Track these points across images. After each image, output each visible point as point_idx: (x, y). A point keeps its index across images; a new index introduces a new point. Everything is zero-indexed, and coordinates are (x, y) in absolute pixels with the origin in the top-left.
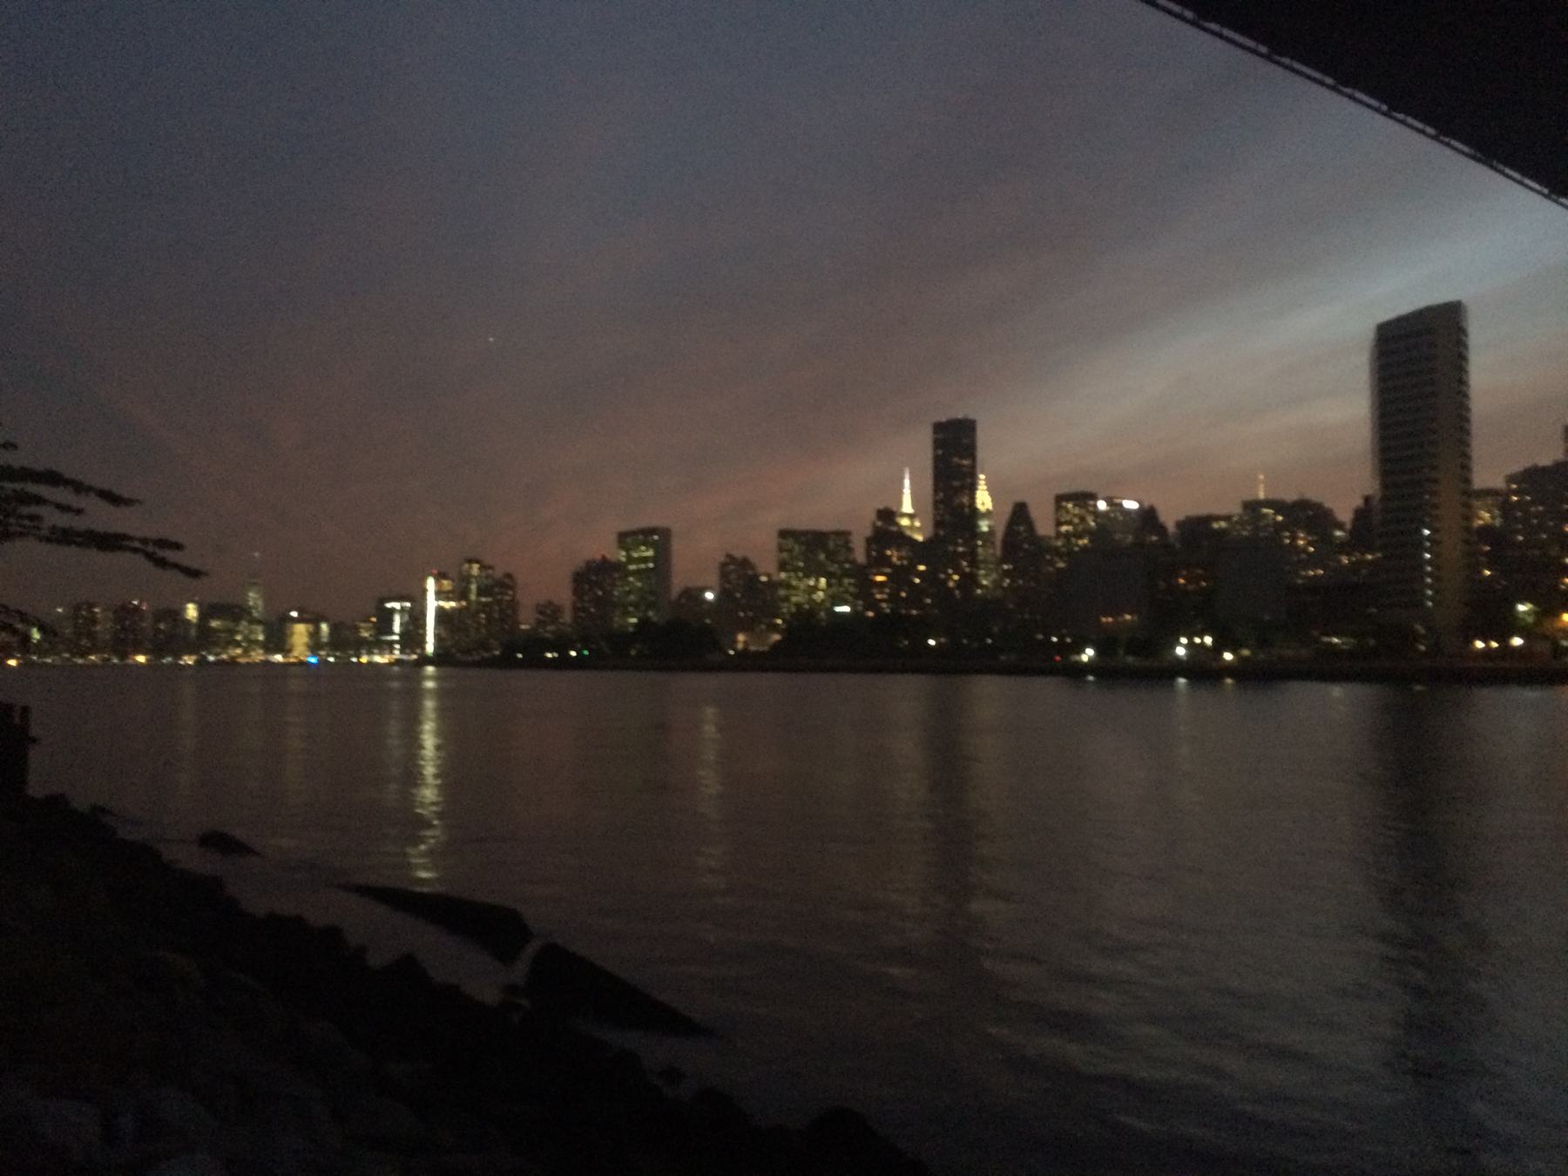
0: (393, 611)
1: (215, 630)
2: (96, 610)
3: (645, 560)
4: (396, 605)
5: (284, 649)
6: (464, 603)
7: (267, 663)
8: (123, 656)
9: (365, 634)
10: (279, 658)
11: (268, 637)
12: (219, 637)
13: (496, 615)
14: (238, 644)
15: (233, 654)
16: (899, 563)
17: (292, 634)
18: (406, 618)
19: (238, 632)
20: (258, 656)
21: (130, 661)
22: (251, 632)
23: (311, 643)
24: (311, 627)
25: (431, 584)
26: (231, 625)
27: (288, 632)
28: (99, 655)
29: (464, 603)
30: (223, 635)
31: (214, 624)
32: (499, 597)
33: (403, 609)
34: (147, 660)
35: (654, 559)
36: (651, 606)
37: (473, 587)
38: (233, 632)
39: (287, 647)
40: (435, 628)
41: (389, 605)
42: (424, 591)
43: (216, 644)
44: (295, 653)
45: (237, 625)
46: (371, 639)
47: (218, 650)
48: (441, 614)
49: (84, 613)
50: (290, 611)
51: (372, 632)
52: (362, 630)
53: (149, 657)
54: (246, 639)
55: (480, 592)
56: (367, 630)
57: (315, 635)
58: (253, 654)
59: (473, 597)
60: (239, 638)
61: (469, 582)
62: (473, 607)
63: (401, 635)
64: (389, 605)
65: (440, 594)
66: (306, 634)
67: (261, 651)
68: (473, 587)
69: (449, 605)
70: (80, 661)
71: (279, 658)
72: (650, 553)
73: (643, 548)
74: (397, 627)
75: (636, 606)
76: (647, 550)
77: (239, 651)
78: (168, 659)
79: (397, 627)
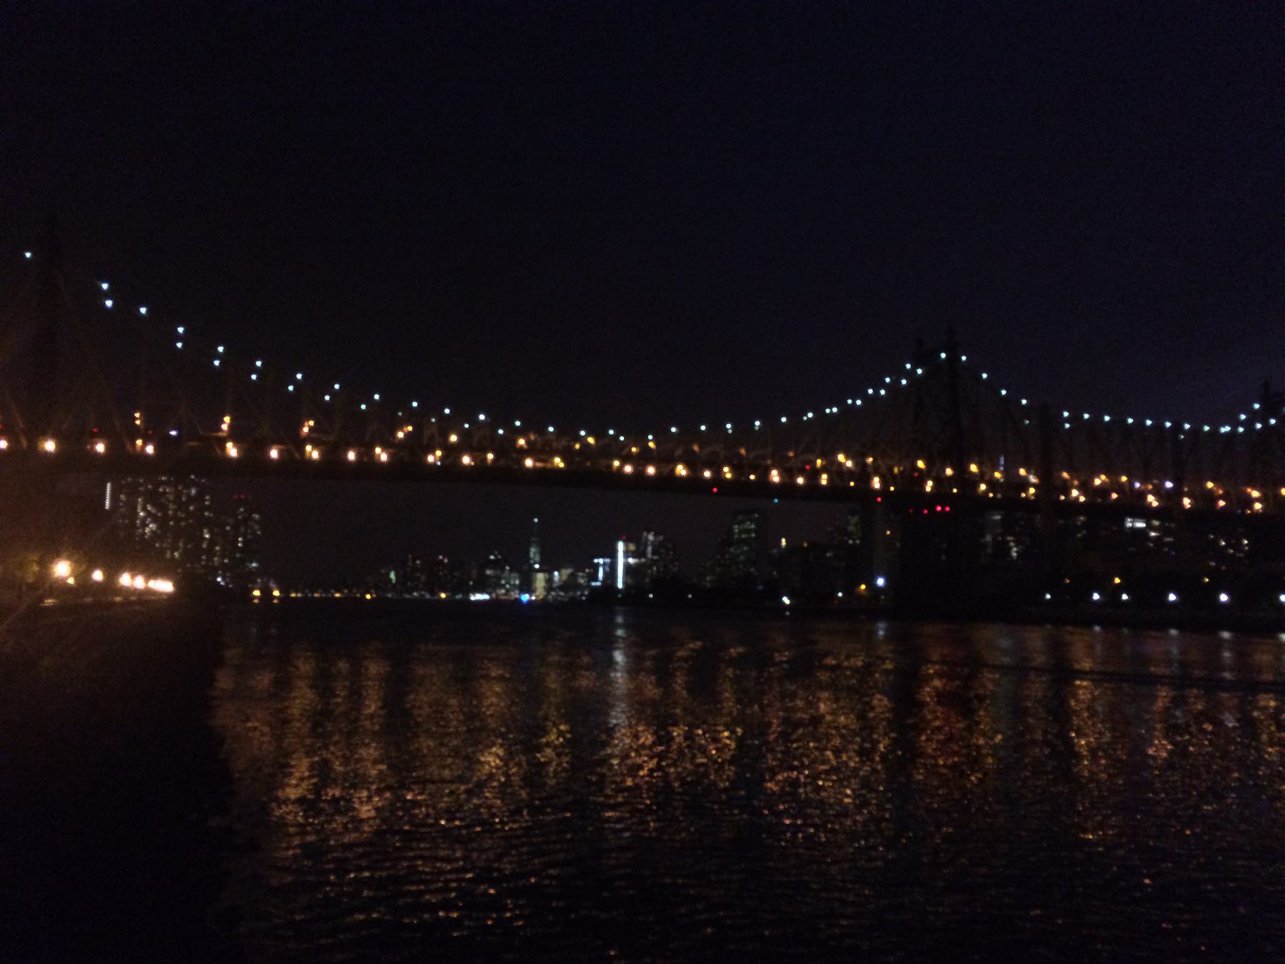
0: (598, 565)
1: (488, 577)
3: (749, 531)
4: (601, 561)
5: (530, 590)
6: (643, 560)
7: (518, 601)
9: (582, 581)
10: (525, 597)
14: (503, 586)
17: (536, 580)
18: (607, 569)
20: (515, 595)
21: (436, 597)
24: (547, 576)
25: (621, 546)
26: (499, 572)
29: (643, 560)
31: (488, 572)
33: (604, 564)
34: (447, 597)
35: (755, 531)
37: (649, 549)
38: (499, 578)
41: (596, 561)
44: (538, 593)
48: (628, 568)
51: (586, 579)
55: (654, 553)
56: (583, 577)
57: (550, 581)
58: (512, 593)
59: (649, 556)
60: (503, 582)
61: (646, 546)
63: (602, 582)
64: (596, 561)
65: (627, 554)
67: (517, 592)
68: (649, 549)
69: (631, 560)
70: (408, 596)
71: (525, 597)
72: (753, 526)
73: (749, 523)
74: (601, 574)
77: (503, 591)
78: (459, 596)
79: (601, 574)
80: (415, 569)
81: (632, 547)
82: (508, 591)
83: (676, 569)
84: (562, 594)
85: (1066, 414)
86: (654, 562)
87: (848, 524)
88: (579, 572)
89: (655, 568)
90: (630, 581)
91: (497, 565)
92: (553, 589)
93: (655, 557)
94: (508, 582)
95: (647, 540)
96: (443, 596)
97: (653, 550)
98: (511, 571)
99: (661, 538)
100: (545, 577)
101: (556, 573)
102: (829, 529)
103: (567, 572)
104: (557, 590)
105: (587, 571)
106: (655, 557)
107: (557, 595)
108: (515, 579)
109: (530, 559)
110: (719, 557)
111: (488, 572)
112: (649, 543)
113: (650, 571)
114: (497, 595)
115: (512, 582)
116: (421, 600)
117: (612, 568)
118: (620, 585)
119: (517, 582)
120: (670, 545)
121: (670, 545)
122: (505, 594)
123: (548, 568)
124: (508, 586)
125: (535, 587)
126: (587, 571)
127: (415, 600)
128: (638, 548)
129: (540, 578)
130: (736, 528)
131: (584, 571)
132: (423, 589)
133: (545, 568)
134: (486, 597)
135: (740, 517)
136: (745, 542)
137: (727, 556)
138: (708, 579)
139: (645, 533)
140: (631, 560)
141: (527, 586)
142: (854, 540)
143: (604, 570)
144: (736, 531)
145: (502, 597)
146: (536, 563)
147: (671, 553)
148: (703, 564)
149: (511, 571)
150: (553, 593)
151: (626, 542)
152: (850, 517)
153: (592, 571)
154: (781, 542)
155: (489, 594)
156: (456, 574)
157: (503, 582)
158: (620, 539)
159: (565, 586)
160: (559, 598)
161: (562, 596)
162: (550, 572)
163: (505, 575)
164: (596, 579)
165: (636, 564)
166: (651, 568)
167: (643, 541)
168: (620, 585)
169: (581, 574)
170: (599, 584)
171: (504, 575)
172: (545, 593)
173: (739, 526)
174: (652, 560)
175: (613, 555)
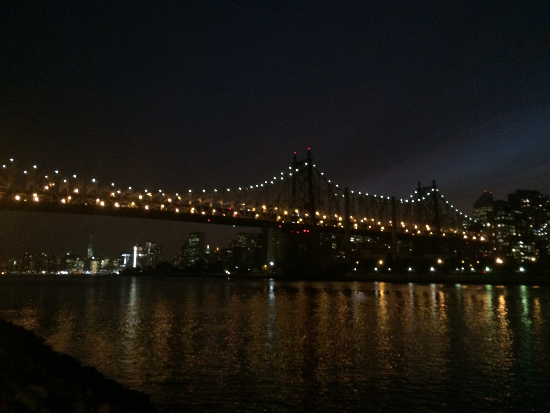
0: (124, 257)
1: (68, 263)
2: (30, 256)
4: (125, 255)
5: (89, 269)
8: (38, 271)
9: (116, 265)
10: (88, 272)
11: (85, 265)
12: (70, 265)
13: (155, 259)
14: (75, 267)
15: (73, 271)
17: (92, 264)
18: (128, 259)
20: (81, 271)
21: (40, 273)
23: (98, 268)
24: (98, 262)
25: (135, 248)
26: (73, 261)
27: (91, 264)
28: (30, 271)
29: (146, 255)
30: (71, 265)
31: (68, 261)
32: (156, 253)
33: (127, 257)
34: (45, 273)
36: (198, 256)
37: (149, 250)
38: (73, 264)
39: (91, 268)
40: (136, 263)
41: (123, 255)
42: (133, 251)
44: (93, 271)
45: (75, 261)
46: (117, 266)
47: (69, 269)
48: (138, 259)
49: (26, 257)
51: (118, 264)
52: (114, 263)
53: (46, 272)
55: (151, 251)
56: (116, 263)
57: (99, 265)
59: (149, 253)
60: (75, 266)
62: (149, 256)
63: (126, 265)
64: (123, 255)
65: (138, 252)
66: (96, 265)
67: (82, 270)
68: (149, 250)
69: (140, 255)
70: (24, 273)
71: (88, 272)
73: (196, 238)
74: (125, 262)
75: (194, 256)
76: (197, 239)
77: (75, 270)
79: (125, 262)
80: (29, 260)
81: (141, 249)
82: (78, 270)
83: (161, 259)
84: (105, 271)
85: (282, 178)
86: (151, 256)
88: (114, 260)
90: (139, 264)
91: (71, 257)
92: (101, 269)
93: (152, 254)
95: (148, 246)
96: (44, 272)
97: (151, 250)
98: (79, 260)
99: (155, 245)
100: (97, 263)
101: (103, 261)
102: (230, 241)
103: (107, 261)
104: (103, 269)
105: (118, 260)
106: (152, 254)
107: (103, 272)
108: (81, 264)
109: (88, 255)
110: (181, 253)
111: (68, 261)
112: (149, 247)
113: (149, 260)
114: (72, 272)
116: (32, 275)
117: (131, 258)
118: (135, 266)
119: (83, 266)
120: (159, 248)
121: (159, 248)
124: (78, 268)
125: (92, 268)
126: (118, 260)
127: (28, 275)
128: (143, 249)
129: (95, 264)
130: (190, 241)
131: (117, 260)
132: (32, 269)
134: (66, 273)
135: (192, 236)
137: (185, 253)
138: (175, 263)
139: (147, 243)
140: (140, 255)
141: (88, 267)
143: (127, 259)
144: (191, 242)
145: (74, 273)
146: (92, 257)
148: (173, 256)
149: (79, 260)
150: (101, 271)
151: (138, 246)
152: (240, 236)
153: (121, 260)
154: (207, 247)
155: (68, 271)
156: (51, 262)
157: (75, 266)
159: (107, 267)
160: (104, 273)
161: (105, 272)
162: (100, 261)
163: (77, 262)
164: (123, 264)
165: (143, 257)
166: (149, 258)
167: (147, 245)
168: (135, 266)
169: (115, 261)
170: (124, 266)
171: (76, 262)
173: (192, 239)
174: (150, 255)
175: (132, 252)
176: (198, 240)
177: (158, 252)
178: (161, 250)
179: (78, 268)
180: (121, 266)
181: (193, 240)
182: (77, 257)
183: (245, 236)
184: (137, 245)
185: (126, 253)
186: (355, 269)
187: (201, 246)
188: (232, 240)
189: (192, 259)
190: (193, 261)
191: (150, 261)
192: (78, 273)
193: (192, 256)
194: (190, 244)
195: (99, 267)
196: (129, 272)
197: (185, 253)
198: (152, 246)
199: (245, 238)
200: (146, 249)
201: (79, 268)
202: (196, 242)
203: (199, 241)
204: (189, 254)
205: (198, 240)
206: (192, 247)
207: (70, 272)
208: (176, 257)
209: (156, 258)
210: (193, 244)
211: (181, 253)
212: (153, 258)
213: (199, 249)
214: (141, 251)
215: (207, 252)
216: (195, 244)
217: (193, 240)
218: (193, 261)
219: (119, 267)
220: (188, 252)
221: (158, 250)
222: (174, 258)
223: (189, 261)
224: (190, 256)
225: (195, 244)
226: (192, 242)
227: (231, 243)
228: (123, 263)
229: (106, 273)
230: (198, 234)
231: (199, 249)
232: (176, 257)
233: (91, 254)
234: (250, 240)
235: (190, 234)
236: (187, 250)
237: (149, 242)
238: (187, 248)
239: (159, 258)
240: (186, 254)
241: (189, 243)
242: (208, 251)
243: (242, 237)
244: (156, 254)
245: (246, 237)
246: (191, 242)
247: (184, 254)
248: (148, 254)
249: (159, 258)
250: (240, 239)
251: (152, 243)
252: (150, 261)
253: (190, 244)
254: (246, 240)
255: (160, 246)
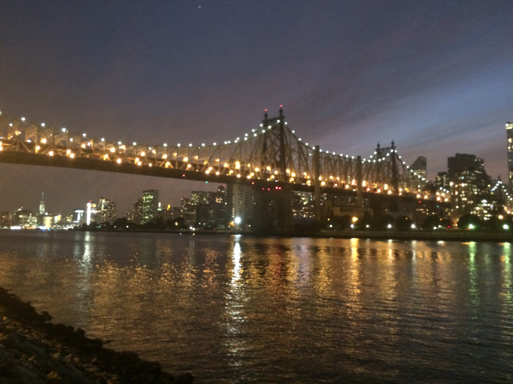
0: (77, 213)
1: (21, 219)
6: (99, 211)
13: (108, 215)
14: (28, 223)
16: (218, 202)
18: (82, 215)
19: (28, 219)
20: (34, 227)
22: (32, 219)
25: (89, 205)
26: (26, 216)
27: (44, 219)
29: (99, 211)
31: (21, 216)
32: (109, 209)
33: (81, 213)
36: (152, 213)
37: (103, 206)
38: (26, 219)
41: (76, 211)
43: (21, 223)
45: (28, 217)
47: (22, 225)
50: (475, 229)
51: (71, 220)
54: (31, 221)
55: (105, 208)
56: (69, 219)
57: (53, 220)
59: (102, 209)
60: (28, 221)
62: (102, 212)
64: (76, 211)
68: (103, 206)
73: (150, 196)
75: (148, 212)
77: (28, 225)
79: (79, 218)
81: (94, 205)
83: (115, 215)
84: (59, 226)
86: (105, 212)
87: (192, 197)
89: (105, 215)
91: (24, 212)
92: (55, 224)
93: (105, 210)
94: (31, 221)
99: (108, 202)
102: (182, 199)
106: (105, 210)
110: (134, 210)
111: (21, 216)
115: (33, 221)
117: (85, 215)
119: (36, 221)
122: (29, 227)
123: (53, 214)
124: (31, 223)
129: (48, 220)
130: (144, 198)
133: (50, 214)
135: (146, 193)
136: (148, 204)
137: (138, 210)
141: (41, 222)
142: (194, 203)
144: (144, 199)
147: (113, 208)
150: (54, 226)
152: (192, 194)
154: (158, 204)
157: (28, 221)
158: (88, 202)
159: (60, 223)
166: (103, 214)
167: (100, 202)
170: (77, 222)
172: (50, 226)
173: (146, 197)
174: (104, 211)
175: (85, 208)
176: (152, 197)
177: (112, 209)
178: (114, 207)
179: (31, 223)
180: (74, 222)
181: (147, 198)
182: (30, 212)
183: (197, 194)
184: (90, 201)
185: (80, 209)
186: (127, 227)
187: (154, 202)
188: (185, 198)
189: (145, 216)
190: (147, 217)
191: (104, 218)
192: (31, 228)
193: (146, 212)
194: (144, 201)
195: (53, 224)
196: (83, 228)
197: (138, 210)
198: (105, 203)
199: (197, 196)
200: (99, 206)
201: (31, 223)
202: (150, 199)
203: (153, 199)
204: (143, 211)
205: (152, 197)
206: (146, 204)
207: (23, 227)
208: (129, 213)
209: (110, 214)
210: (147, 201)
211: (134, 210)
212: (107, 215)
213: (153, 206)
214: (94, 208)
215: (159, 210)
216: (149, 201)
217: (147, 198)
218: (147, 217)
219: (72, 223)
220: (142, 209)
221: (112, 207)
222: (127, 214)
223: (143, 218)
224: (145, 213)
225: (149, 201)
226: (146, 200)
227: (182, 201)
228: (76, 219)
229: (59, 229)
230: (152, 192)
231: (153, 206)
232: (129, 213)
233: (43, 210)
234: (203, 198)
235: (145, 192)
236: (140, 207)
237: (103, 198)
238: (141, 206)
239: (113, 214)
240: (139, 211)
241: (143, 200)
242: (160, 208)
243: (195, 195)
244: (110, 211)
245: (198, 196)
246: (144, 199)
247: (137, 211)
248: (101, 211)
249: (113, 214)
250: (192, 197)
251: (106, 200)
252: (104, 218)
253: (144, 201)
254: (199, 198)
255: (113, 203)
